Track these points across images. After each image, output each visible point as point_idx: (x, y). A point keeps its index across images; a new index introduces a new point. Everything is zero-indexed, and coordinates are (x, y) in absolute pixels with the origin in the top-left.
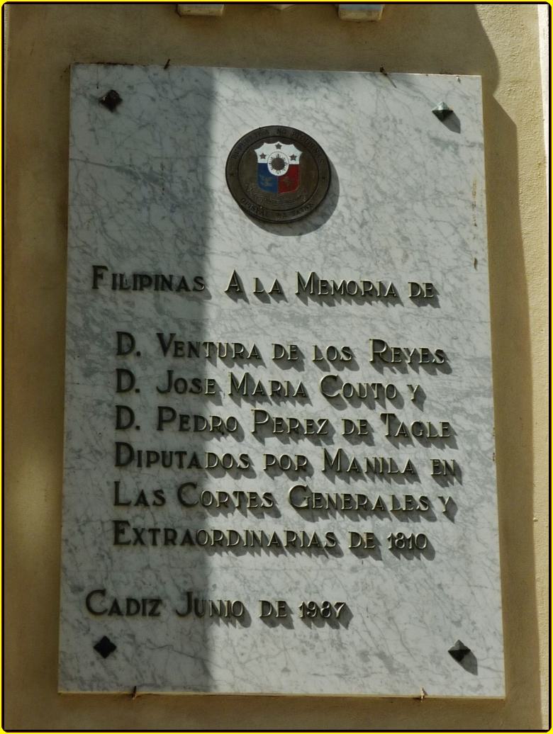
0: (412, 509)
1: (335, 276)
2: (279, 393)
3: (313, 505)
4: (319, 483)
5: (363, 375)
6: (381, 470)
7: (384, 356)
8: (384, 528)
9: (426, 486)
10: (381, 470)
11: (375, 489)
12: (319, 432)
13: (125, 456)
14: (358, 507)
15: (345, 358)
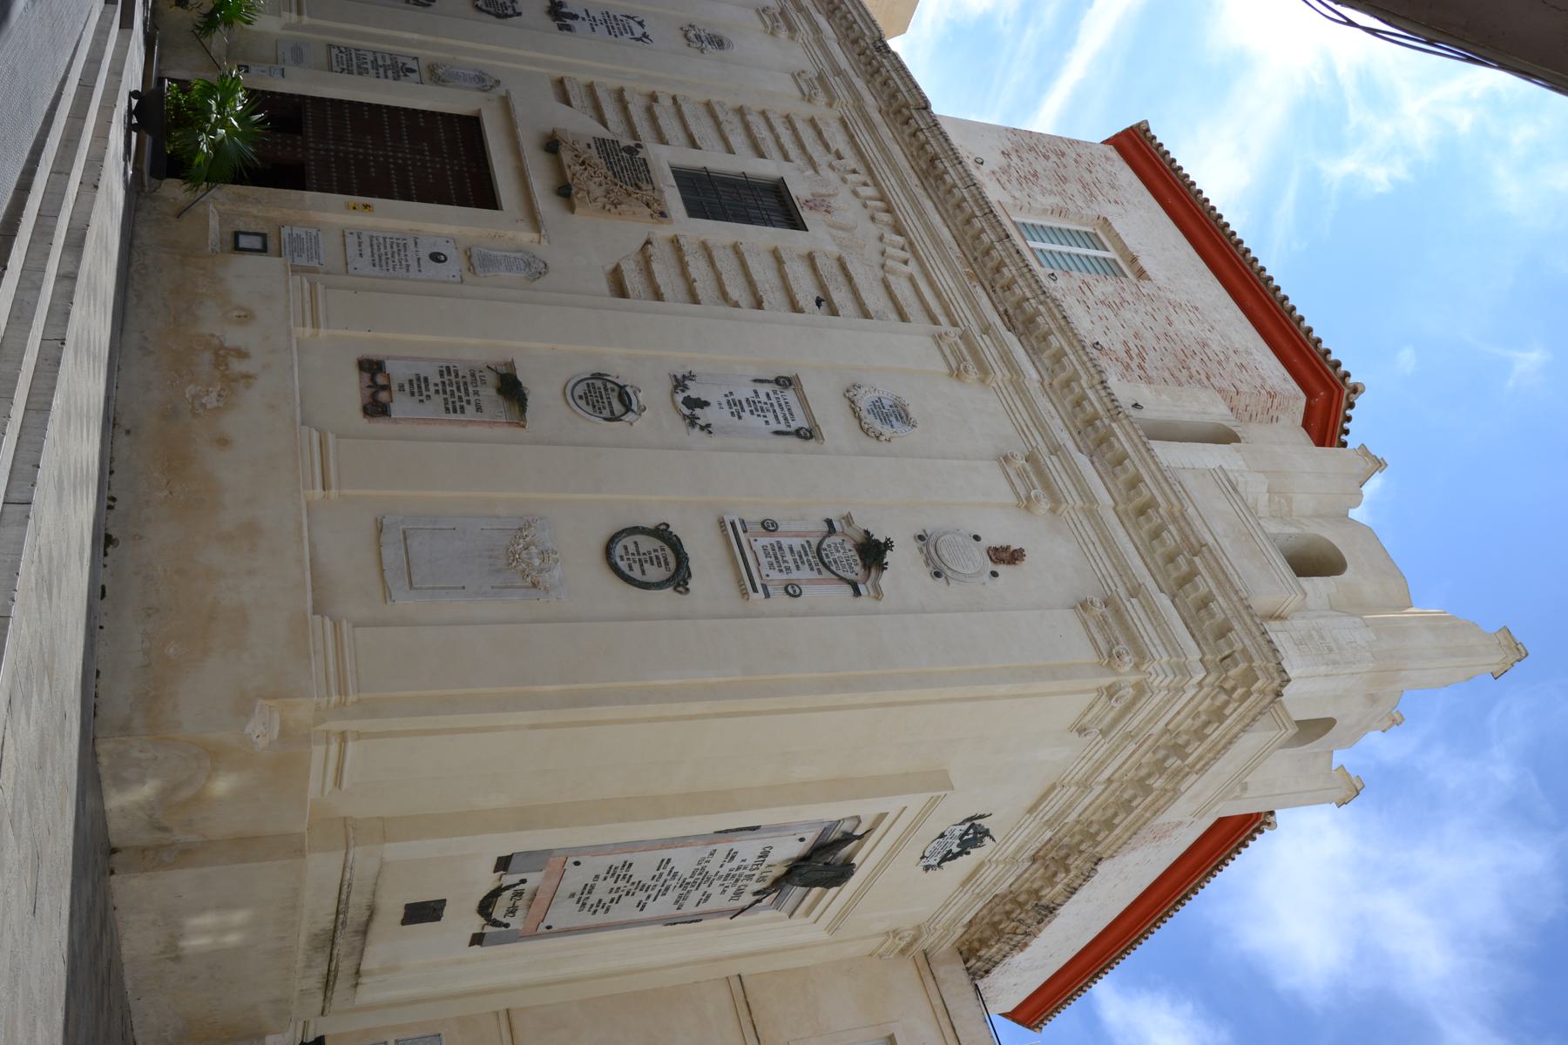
0: (381, 266)
1: (421, 261)
2: (399, 255)
3: (380, 257)
4: (383, 258)
5: (404, 263)
6: (387, 263)
7: (408, 266)
8: (377, 261)
9: (384, 267)
10: (387, 263)
11: (383, 262)
12: (393, 256)
13: (385, 238)
14: (380, 260)
15: (407, 261)
